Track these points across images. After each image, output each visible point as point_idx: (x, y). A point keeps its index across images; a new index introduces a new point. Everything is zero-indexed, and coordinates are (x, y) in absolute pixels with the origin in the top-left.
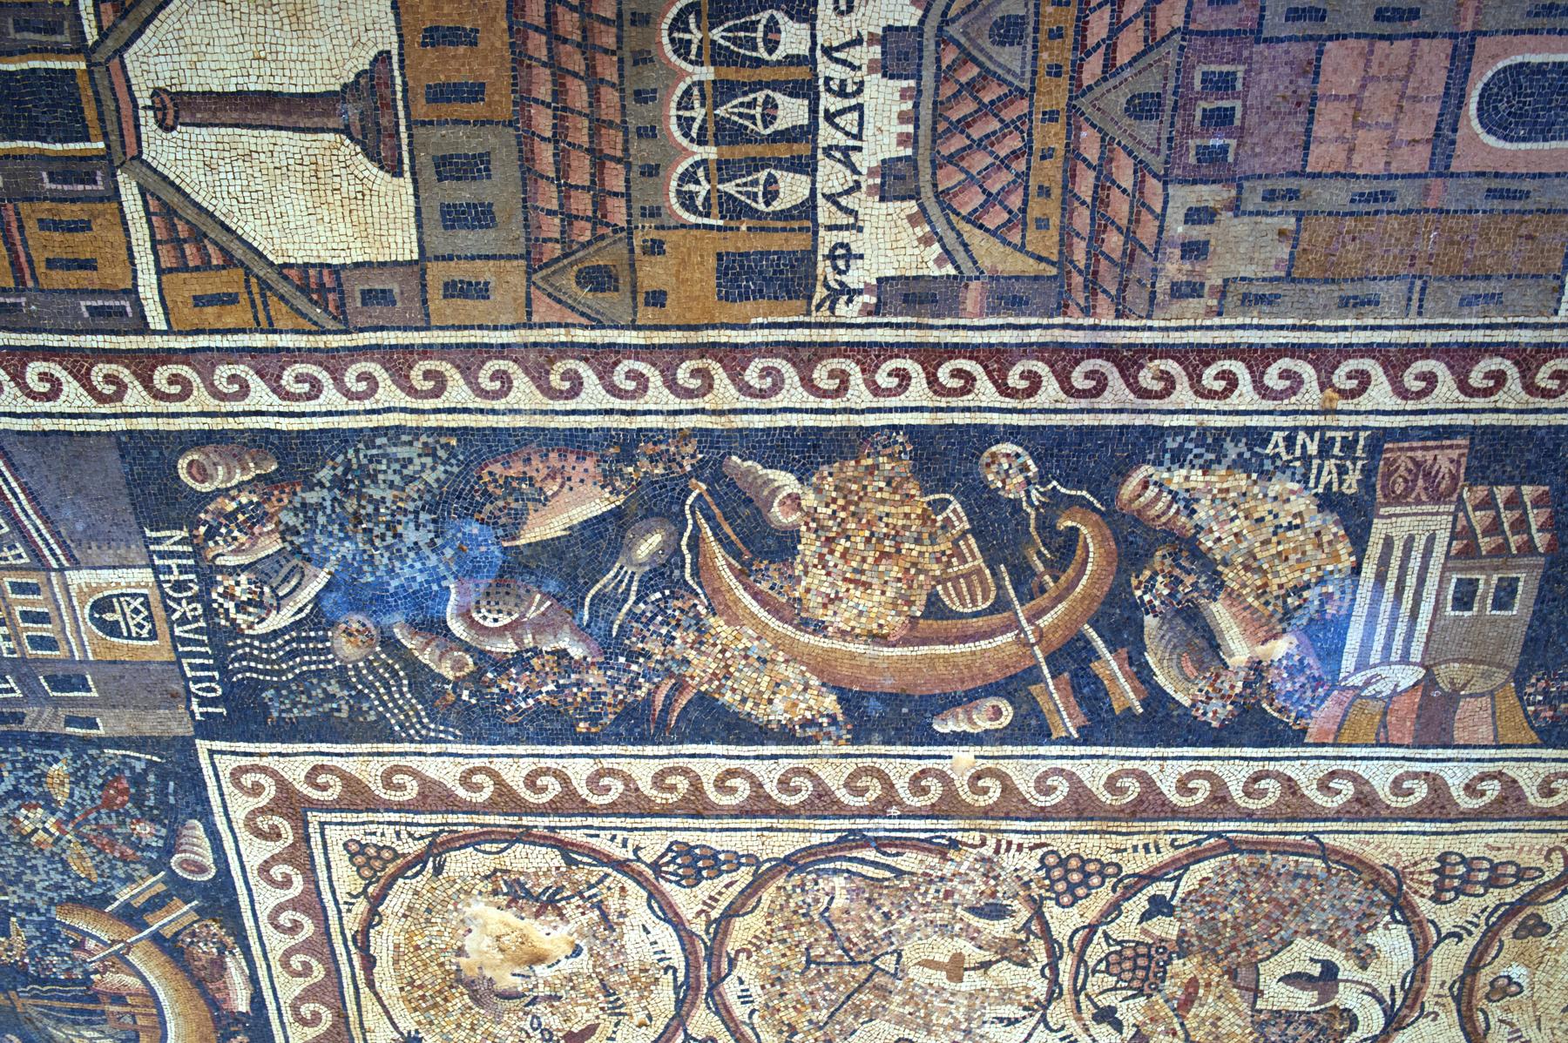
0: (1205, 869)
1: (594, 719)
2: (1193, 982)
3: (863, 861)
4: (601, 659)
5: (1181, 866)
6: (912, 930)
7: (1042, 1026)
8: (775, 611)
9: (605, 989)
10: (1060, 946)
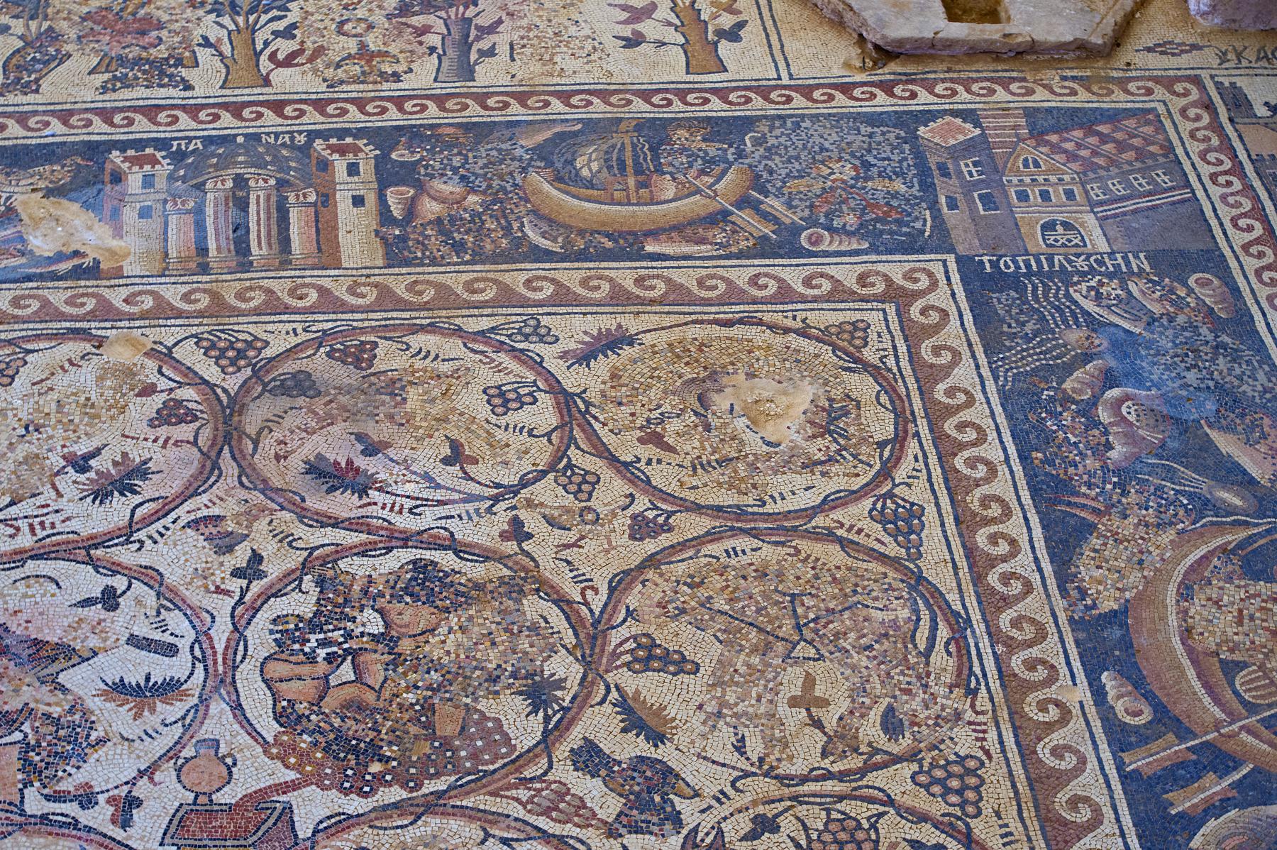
3: (934, 628)
4: (1111, 467)
6: (854, 668)
7: (736, 774)
8: (1192, 569)
9: (724, 462)
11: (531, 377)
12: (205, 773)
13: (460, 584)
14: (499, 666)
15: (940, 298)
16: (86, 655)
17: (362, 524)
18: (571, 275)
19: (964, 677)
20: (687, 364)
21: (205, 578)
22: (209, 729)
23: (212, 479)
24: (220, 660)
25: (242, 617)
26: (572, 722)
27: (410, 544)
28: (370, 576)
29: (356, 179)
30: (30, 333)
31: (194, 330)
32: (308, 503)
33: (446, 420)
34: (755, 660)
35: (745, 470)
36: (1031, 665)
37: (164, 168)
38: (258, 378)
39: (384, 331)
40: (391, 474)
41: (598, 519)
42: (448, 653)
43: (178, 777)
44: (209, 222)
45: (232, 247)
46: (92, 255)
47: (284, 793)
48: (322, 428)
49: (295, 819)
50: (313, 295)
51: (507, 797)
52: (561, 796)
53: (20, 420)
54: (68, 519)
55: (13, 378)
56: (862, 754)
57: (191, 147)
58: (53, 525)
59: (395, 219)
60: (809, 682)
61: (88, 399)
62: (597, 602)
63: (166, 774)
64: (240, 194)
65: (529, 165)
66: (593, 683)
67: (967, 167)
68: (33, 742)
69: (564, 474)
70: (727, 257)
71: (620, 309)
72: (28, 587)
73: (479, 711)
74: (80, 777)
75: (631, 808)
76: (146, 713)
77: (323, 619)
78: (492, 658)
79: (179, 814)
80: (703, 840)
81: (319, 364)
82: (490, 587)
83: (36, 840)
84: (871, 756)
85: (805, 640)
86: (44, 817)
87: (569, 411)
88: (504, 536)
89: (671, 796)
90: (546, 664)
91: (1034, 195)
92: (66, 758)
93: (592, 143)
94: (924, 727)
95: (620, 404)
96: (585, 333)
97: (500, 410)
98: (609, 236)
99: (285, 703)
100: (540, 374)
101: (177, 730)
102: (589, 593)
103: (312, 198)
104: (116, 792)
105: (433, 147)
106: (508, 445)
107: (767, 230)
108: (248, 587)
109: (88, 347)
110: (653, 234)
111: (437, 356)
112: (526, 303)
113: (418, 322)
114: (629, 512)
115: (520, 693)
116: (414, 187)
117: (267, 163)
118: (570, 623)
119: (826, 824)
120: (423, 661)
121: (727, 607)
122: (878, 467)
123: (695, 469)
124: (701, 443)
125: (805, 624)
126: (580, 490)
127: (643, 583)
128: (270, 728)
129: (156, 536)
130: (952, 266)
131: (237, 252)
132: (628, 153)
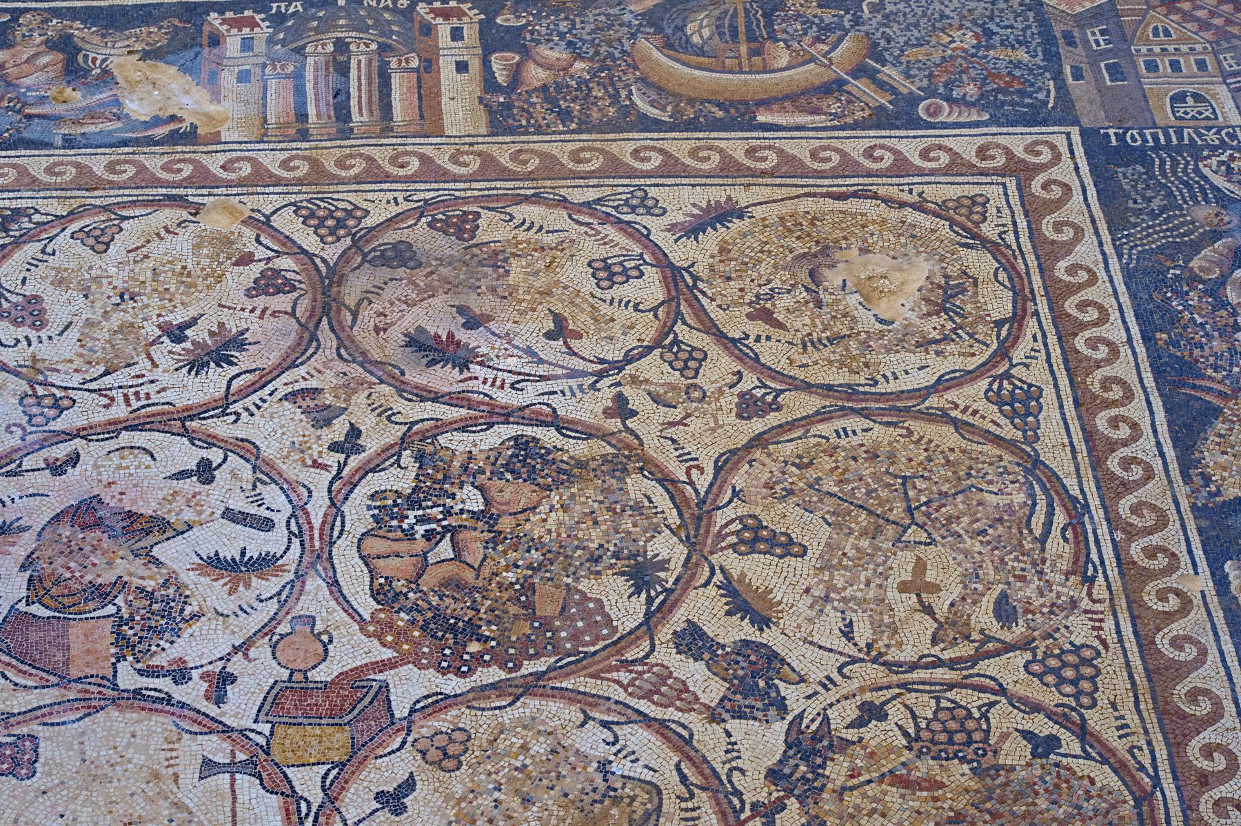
0: (1105, 777)
1: (1173, 343)
2: (942, 785)
3: (1050, 514)
5: (1107, 757)
6: (966, 553)
7: (843, 659)
9: (835, 339)
10: (972, 667)
11: (638, 250)
12: (301, 651)
13: (562, 461)
14: (601, 546)
15: (1064, 172)
16: (181, 528)
17: (463, 399)
18: (680, 146)
19: (1081, 563)
20: (798, 238)
21: (302, 452)
22: (305, 606)
23: (310, 351)
24: (317, 536)
25: (339, 492)
26: (675, 604)
27: (511, 419)
28: (470, 452)
29: (460, 44)
30: (125, 199)
31: (293, 198)
32: (408, 377)
33: (549, 293)
34: (865, 543)
35: (857, 349)
36: (1151, 553)
37: (264, 30)
38: (358, 248)
39: (488, 201)
40: (493, 348)
41: (704, 397)
42: (549, 531)
43: (273, 653)
44: (309, 87)
45: (332, 113)
46: (189, 119)
47: (381, 671)
48: (422, 300)
49: (392, 698)
50: (415, 164)
51: (608, 679)
52: (663, 680)
53: (115, 288)
54: (164, 389)
55: (108, 245)
56: (973, 641)
57: (291, 10)
58: (148, 396)
59: (500, 86)
60: (920, 567)
61: (184, 268)
62: (703, 482)
63: (261, 650)
64: (341, 58)
65: (638, 31)
66: (697, 565)
67: (1094, 35)
68: (126, 616)
69: (670, 351)
70: (842, 128)
71: (730, 181)
72: (122, 458)
73: (581, 591)
74: (173, 652)
75: (735, 693)
76: (241, 588)
77: (422, 495)
78: (594, 537)
79: (274, 692)
80: (808, 727)
81: (420, 234)
82: (593, 465)
83: (128, 715)
84: (983, 643)
85: (916, 524)
86: (137, 692)
87: (676, 285)
88: (607, 413)
89: (776, 681)
90: (649, 544)
91: (1164, 65)
92: (160, 633)
93: (704, 8)
94: (1038, 615)
95: (729, 279)
96: (694, 205)
97: (605, 284)
98: (719, 105)
99: (382, 580)
100: (646, 247)
101: (273, 606)
102: (694, 472)
103: (415, 63)
104: (210, 667)
105: (540, 12)
106: (613, 320)
107: (884, 100)
108: (345, 462)
109: (185, 214)
110: (765, 103)
111: (541, 228)
112: (632, 174)
113: (522, 192)
114: (737, 390)
115: (623, 574)
116: (519, 53)
117: (369, 27)
118: (674, 503)
119: (935, 713)
120: (524, 539)
121: (836, 489)
122: (995, 346)
123: (805, 346)
124: (812, 320)
125: (917, 508)
126: (686, 367)
127: (750, 462)
128: (367, 606)
129: (253, 408)
130: (1077, 139)
131: (337, 118)
132: (741, 20)
